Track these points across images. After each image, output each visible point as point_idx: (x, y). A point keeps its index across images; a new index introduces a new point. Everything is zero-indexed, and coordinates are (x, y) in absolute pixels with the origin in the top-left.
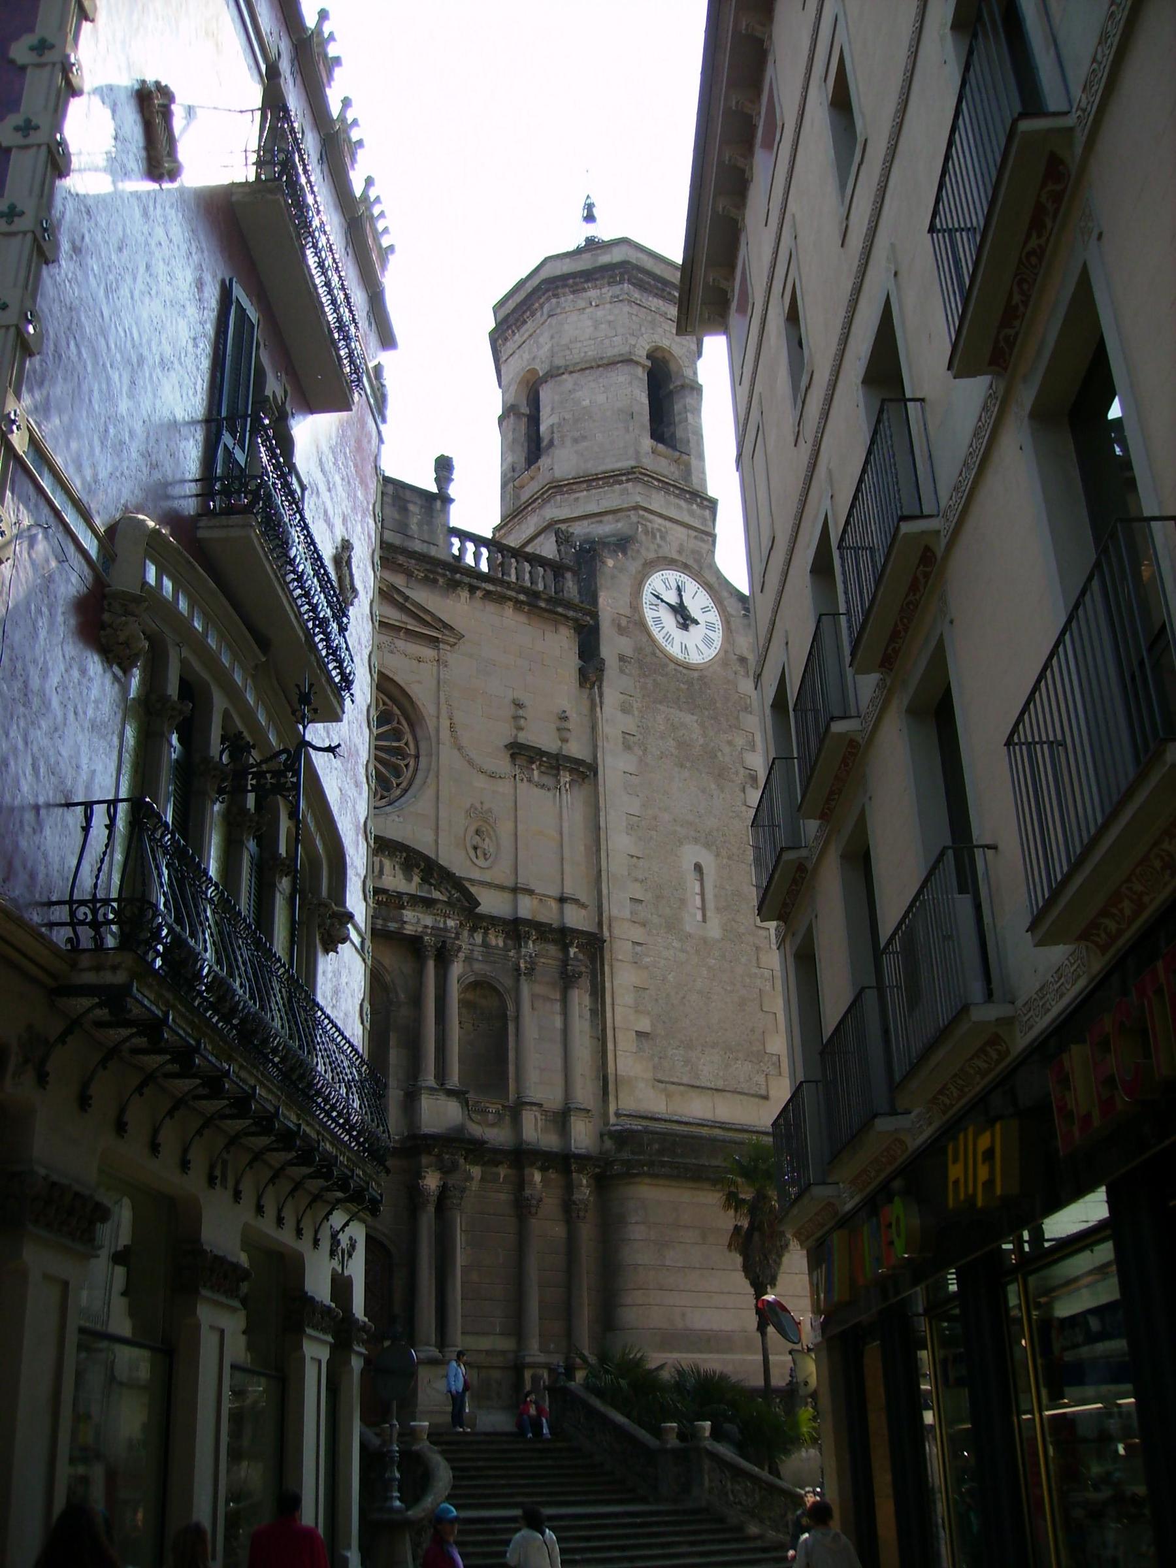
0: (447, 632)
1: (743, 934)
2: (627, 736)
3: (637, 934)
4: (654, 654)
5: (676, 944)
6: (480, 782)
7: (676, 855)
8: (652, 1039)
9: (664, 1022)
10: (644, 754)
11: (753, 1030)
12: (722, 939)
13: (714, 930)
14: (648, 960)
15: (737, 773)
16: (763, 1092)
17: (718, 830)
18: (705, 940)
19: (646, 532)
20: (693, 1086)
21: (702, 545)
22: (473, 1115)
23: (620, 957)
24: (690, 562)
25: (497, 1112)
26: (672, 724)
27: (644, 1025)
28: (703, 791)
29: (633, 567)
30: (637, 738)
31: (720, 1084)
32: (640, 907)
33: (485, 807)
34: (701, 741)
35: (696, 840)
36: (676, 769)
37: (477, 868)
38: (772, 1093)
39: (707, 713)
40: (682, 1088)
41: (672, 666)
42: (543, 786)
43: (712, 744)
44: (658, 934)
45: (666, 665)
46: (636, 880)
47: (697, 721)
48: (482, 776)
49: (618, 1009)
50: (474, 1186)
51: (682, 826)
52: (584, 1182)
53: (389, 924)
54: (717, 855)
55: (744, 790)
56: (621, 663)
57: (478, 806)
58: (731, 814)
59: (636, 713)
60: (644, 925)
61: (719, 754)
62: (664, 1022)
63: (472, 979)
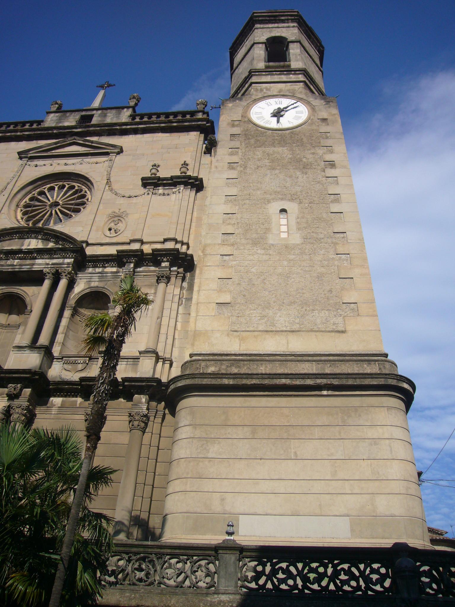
0: (111, 148)
1: (323, 238)
2: (232, 164)
3: (227, 250)
4: (257, 130)
5: (263, 252)
6: (122, 201)
7: (265, 208)
8: (232, 306)
9: (244, 296)
10: (244, 169)
11: (330, 291)
12: (302, 243)
13: (296, 239)
14: (235, 263)
15: (318, 165)
16: (341, 328)
17: (301, 192)
18: (287, 247)
19: (257, 90)
20: (267, 331)
21: (296, 87)
22: (66, 366)
23: (209, 264)
24: (287, 94)
25: (84, 362)
26: (268, 154)
27: (226, 298)
28: (291, 177)
29: (244, 103)
30: (239, 163)
31: (296, 327)
32: (231, 237)
33: (121, 211)
34: (290, 156)
35: (282, 199)
36: (269, 171)
37: (108, 238)
38: (348, 328)
39: (295, 145)
40: (256, 333)
41: (271, 131)
42: (164, 194)
43: (299, 156)
44: (244, 249)
45: (266, 132)
46: (229, 224)
47: (287, 149)
48: (122, 198)
49: (202, 293)
50: (54, 411)
51: (271, 194)
52: (144, 400)
53: (23, 267)
54: (301, 203)
55: (324, 171)
56: (232, 138)
57: (117, 211)
58: (313, 183)
59: (240, 154)
60: (233, 245)
61: (304, 160)
62: (244, 296)
63: (88, 291)
